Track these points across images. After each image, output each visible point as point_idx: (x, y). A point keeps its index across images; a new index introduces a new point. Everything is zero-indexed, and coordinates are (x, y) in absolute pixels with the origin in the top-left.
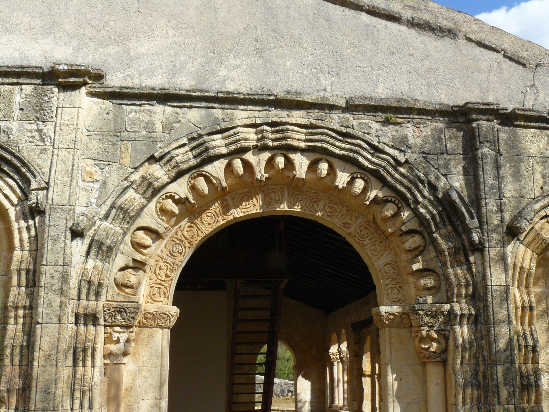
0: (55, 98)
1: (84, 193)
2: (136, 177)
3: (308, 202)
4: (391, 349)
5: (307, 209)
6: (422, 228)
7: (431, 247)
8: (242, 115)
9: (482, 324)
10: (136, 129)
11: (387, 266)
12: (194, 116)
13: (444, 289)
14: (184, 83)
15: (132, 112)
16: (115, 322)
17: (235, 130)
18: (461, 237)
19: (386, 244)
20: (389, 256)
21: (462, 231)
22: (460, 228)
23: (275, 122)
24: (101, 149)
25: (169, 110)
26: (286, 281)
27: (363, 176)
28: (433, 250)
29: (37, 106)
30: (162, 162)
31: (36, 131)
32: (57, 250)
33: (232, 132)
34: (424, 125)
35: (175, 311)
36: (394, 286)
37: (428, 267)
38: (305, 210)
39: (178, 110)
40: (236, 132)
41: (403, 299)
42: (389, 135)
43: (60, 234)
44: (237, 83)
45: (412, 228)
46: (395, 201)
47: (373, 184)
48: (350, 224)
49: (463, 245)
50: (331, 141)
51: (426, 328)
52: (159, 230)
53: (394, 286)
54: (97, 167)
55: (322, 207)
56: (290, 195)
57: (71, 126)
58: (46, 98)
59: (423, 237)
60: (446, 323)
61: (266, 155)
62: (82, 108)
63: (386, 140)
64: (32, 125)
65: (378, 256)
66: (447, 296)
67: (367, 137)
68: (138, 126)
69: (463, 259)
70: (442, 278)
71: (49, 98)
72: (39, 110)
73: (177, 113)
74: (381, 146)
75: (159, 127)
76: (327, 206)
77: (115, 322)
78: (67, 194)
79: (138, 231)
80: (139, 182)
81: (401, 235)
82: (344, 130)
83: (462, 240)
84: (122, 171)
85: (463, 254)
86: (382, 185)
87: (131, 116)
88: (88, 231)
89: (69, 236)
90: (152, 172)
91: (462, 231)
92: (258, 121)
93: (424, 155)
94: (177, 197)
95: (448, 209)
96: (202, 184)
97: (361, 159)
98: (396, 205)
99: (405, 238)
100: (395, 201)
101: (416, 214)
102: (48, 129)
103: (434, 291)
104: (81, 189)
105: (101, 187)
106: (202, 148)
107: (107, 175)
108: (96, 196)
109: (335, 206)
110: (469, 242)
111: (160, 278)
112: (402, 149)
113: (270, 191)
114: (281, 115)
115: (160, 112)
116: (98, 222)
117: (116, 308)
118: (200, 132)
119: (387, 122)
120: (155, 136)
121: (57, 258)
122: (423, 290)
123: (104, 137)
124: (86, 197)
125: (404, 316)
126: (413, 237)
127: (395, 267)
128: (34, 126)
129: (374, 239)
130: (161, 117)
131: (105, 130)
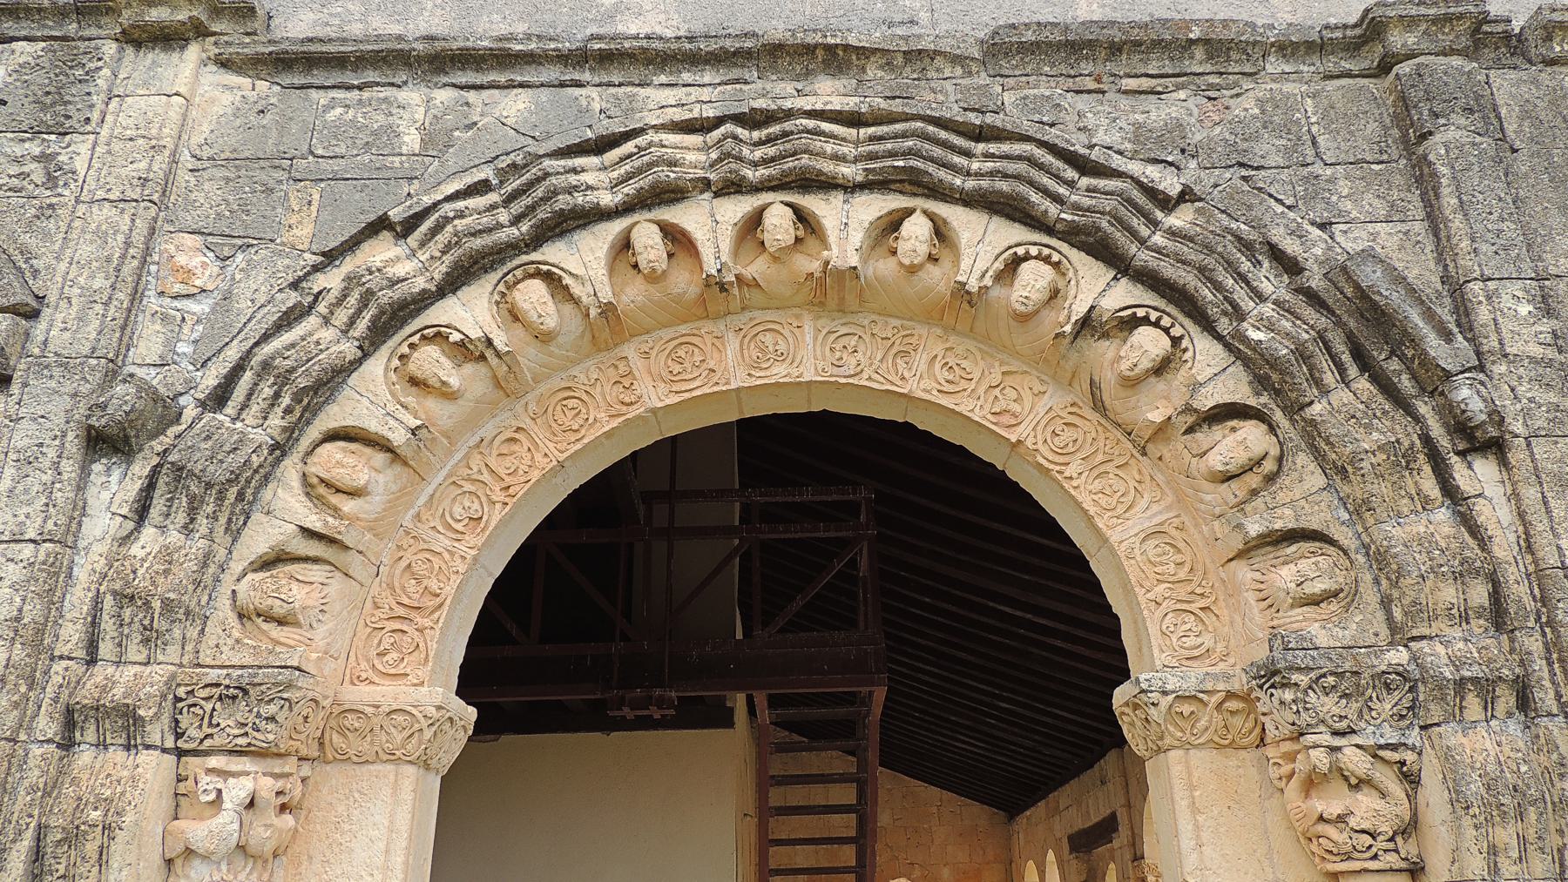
0: (106, 72)
1: (158, 327)
2: (331, 280)
3: (879, 357)
4: (1197, 827)
5: (875, 376)
6: (1264, 399)
7: (1303, 459)
8: (661, 99)
9: (1550, 714)
10: (341, 150)
11: (1152, 543)
13: (1370, 596)
15: (334, 106)
16: (211, 736)
17: (641, 141)
18: (1410, 411)
19: (1140, 472)
20: (1155, 508)
21: (1413, 392)
22: (1406, 384)
23: (762, 111)
24: (228, 204)
25: (444, 96)
26: (880, 694)
27: (1046, 251)
28: (1313, 466)
29: (48, 93)
30: (413, 240)
31: (36, 159)
32: (26, 491)
33: (629, 147)
34: (1234, 92)
35: (472, 713)
36: (1184, 606)
37: (1303, 524)
38: (870, 378)
39: (471, 96)
40: (643, 144)
41: (1220, 647)
42: (1121, 123)
43: (47, 442)
45: (1228, 399)
46: (1159, 319)
47: (1081, 273)
48: (1014, 415)
49: (1427, 440)
50: (937, 152)
51: (1327, 739)
52: (390, 435)
53: (1184, 606)
54: (211, 254)
55: (923, 367)
56: (820, 338)
57: (141, 141)
58: (79, 72)
59: (1272, 429)
60: (1402, 717)
61: (735, 209)
63: (1114, 138)
64: (27, 145)
65: (1120, 510)
66: (1390, 618)
67: (1052, 135)
68: (349, 142)
69: (1431, 487)
70: (1361, 559)
71: (87, 73)
72: (53, 104)
73: (467, 104)
74: (1095, 155)
75: (411, 140)
76: (938, 366)
77: (211, 736)
78: (95, 324)
79: (328, 446)
80: (335, 293)
81: (1190, 430)
82: (975, 119)
83: (1417, 419)
84: (287, 261)
85: (1427, 469)
86: (1112, 273)
87: (332, 115)
88: (154, 435)
89: (73, 443)
90: (379, 264)
91: (1413, 392)
92: (710, 112)
93: (1244, 173)
94: (455, 337)
95: (1352, 324)
96: (532, 296)
97: (1035, 197)
98: (1166, 331)
99: (1203, 437)
100: (1159, 319)
101: (1235, 347)
103: (1334, 606)
104: (148, 316)
105: (213, 311)
106: (540, 192)
107: (238, 277)
108: (195, 335)
109: (964, 364)
110: (1446, 425)
111: (406, 601)
112: (1170, 159)
113: (761, 328)
114: (779, 91)
115: (415, 105)
116: (190, 413)
117: (218, 685)
118: (534, 148)
120: (397, 165)
121: (22, 518)
122: (1292, 606)
123: (243, 172)
124: (161, 339)
125: (1233, 705)
126: (1233, 430)
127: (1181, 545)
128: (35, 148)
129: (1100, 457)
130: (419, 116)
131: (247, 154)
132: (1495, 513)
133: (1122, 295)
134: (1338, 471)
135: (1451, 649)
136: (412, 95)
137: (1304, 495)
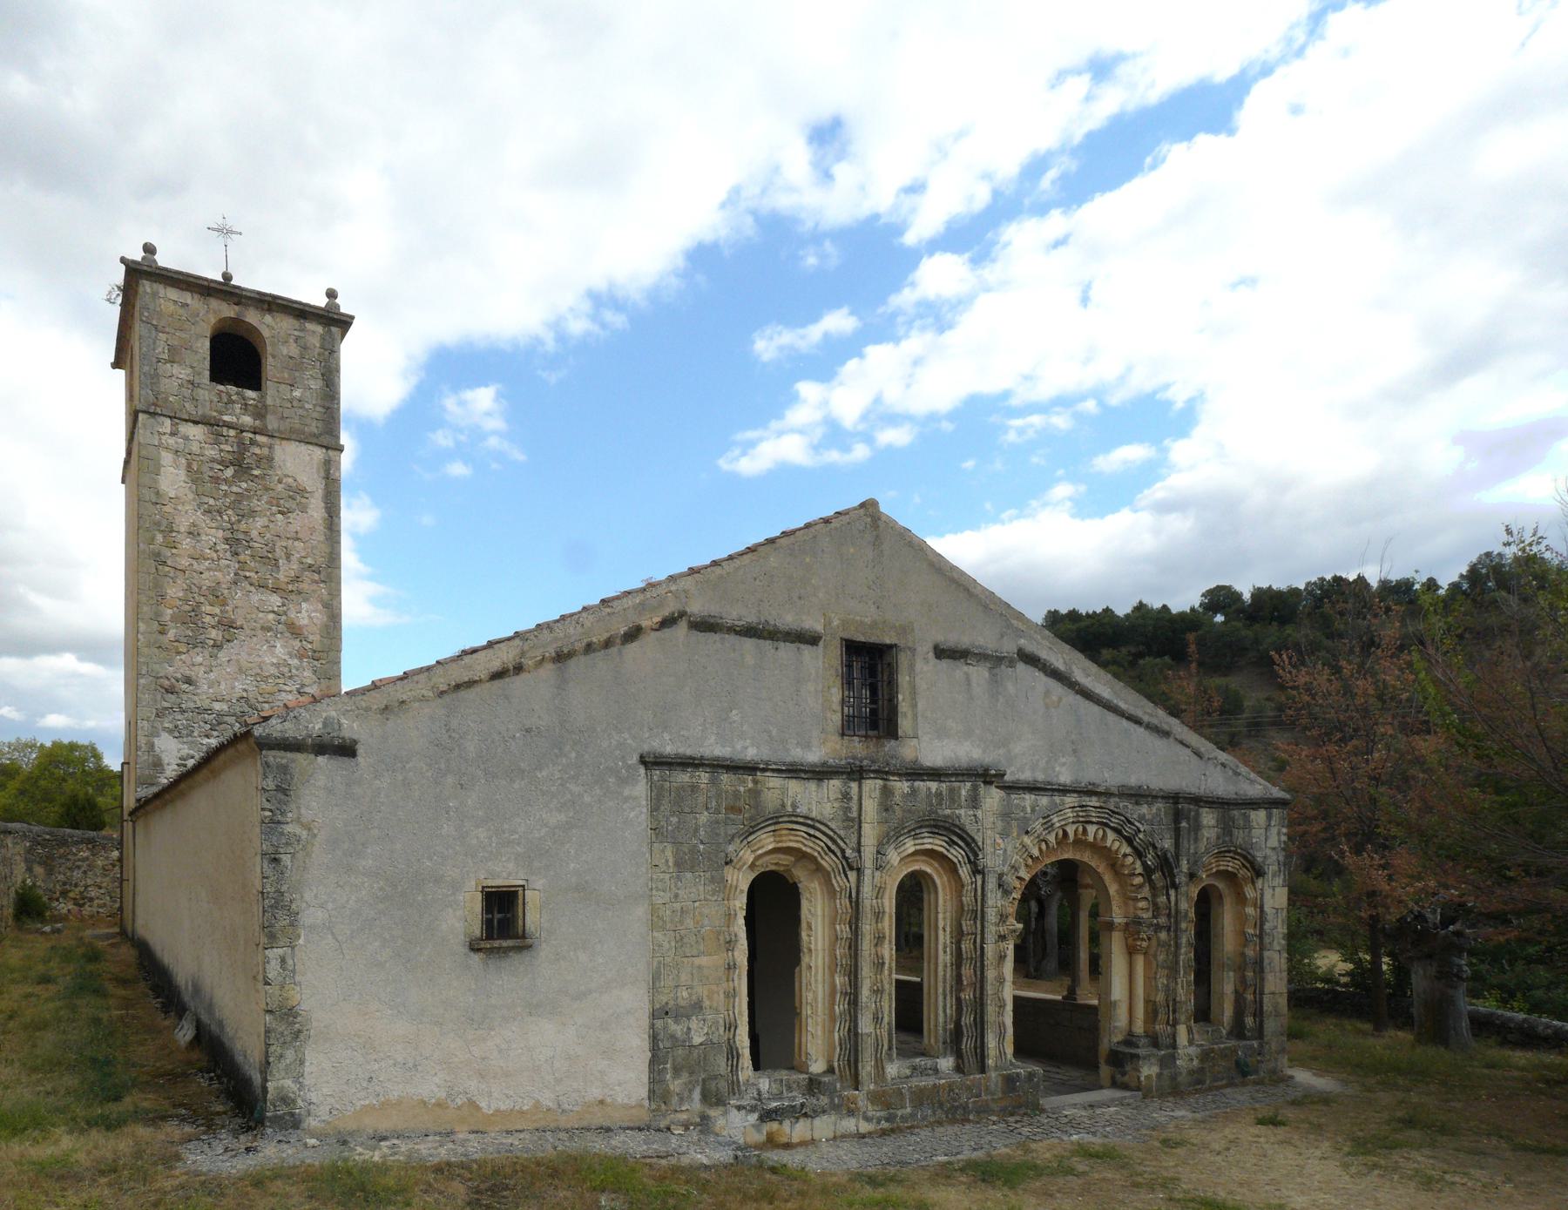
8: (1071, 800)
12: (1044, 801)
14: (1040, 777)
44: (1065, 778)
62: (993, 798)
101: (1144, 864)
102: (979, 813)
114: (1087, 801)
115: (1029, 799)
119: (1137, 803)
132: (1173, 898)
133: (1128, 850)
134: (1153, 887)
135: (1162, 920)
136: (1027, 796)
137: (1146, 892)
